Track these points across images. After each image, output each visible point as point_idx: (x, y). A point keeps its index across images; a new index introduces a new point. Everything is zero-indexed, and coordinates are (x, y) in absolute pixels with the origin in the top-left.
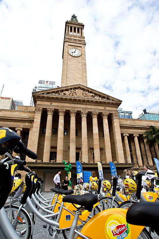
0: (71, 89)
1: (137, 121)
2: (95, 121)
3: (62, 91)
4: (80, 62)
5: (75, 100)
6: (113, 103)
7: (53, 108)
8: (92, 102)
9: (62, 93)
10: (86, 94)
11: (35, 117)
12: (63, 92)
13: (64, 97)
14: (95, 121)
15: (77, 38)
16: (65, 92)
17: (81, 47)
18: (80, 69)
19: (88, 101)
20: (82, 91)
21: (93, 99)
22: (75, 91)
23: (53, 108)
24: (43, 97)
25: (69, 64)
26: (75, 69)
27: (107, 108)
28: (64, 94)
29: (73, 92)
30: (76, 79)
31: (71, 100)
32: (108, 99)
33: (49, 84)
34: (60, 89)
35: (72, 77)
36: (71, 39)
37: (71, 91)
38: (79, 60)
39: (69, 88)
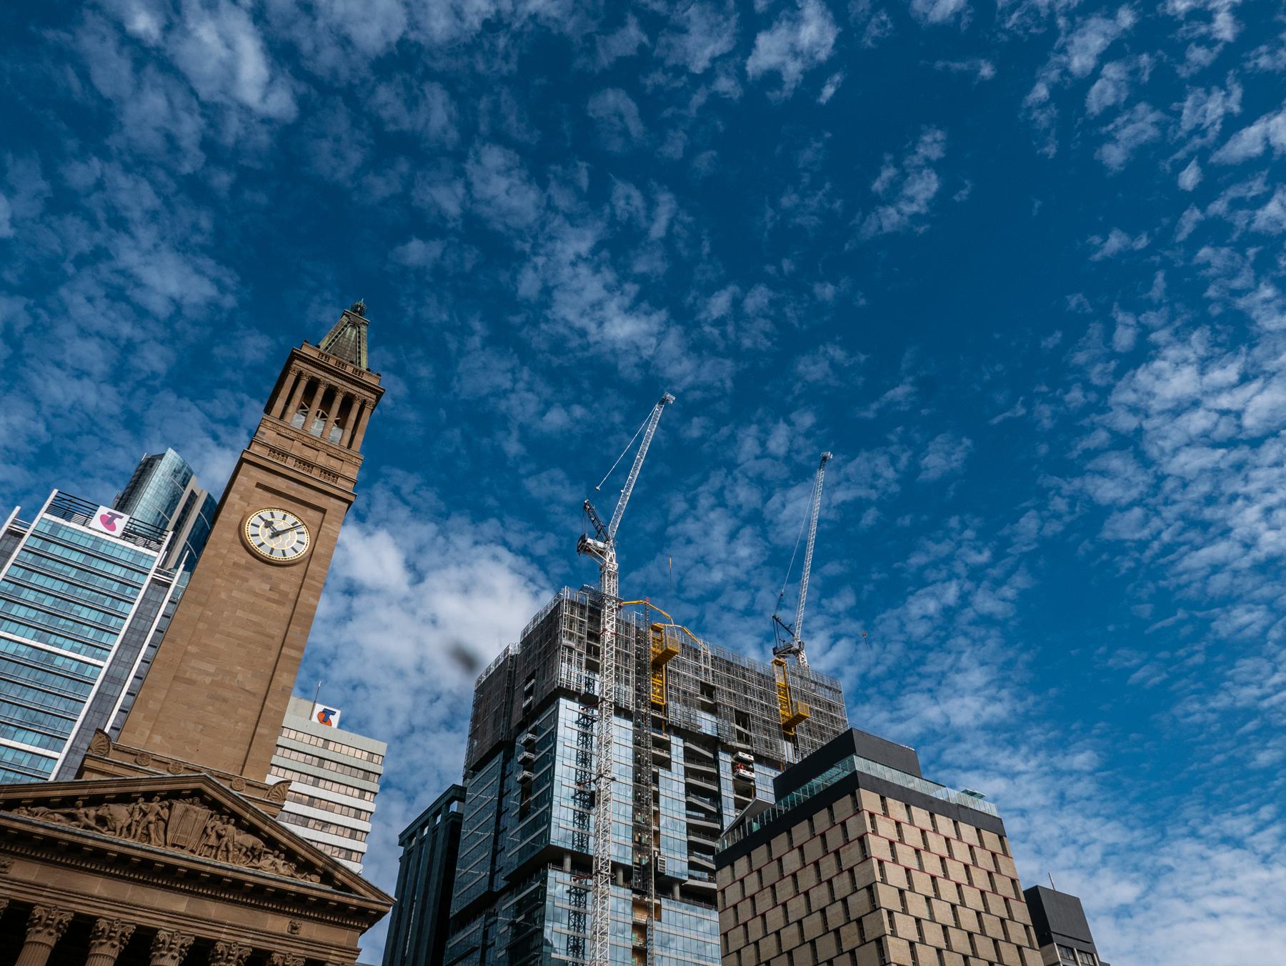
0: (149, 797)
4: (285, 594)
6: (342, 909)
9: (92, 812)
15: (322, 460)
16: (111, 806)
18: (272, 637)
22: (165, 813)
23: (8, 892)
25: (223, 596)
26: (241, 632)
27: (309, 930)
28: (101, 821)
29: (152, 818)
30: (228, 694)
32: (327, 878)
33: (118, 532)
34: (86, 792)
35: (208, 680)
36: (285, 455)
38: (283, 587)
39: (141, 789)
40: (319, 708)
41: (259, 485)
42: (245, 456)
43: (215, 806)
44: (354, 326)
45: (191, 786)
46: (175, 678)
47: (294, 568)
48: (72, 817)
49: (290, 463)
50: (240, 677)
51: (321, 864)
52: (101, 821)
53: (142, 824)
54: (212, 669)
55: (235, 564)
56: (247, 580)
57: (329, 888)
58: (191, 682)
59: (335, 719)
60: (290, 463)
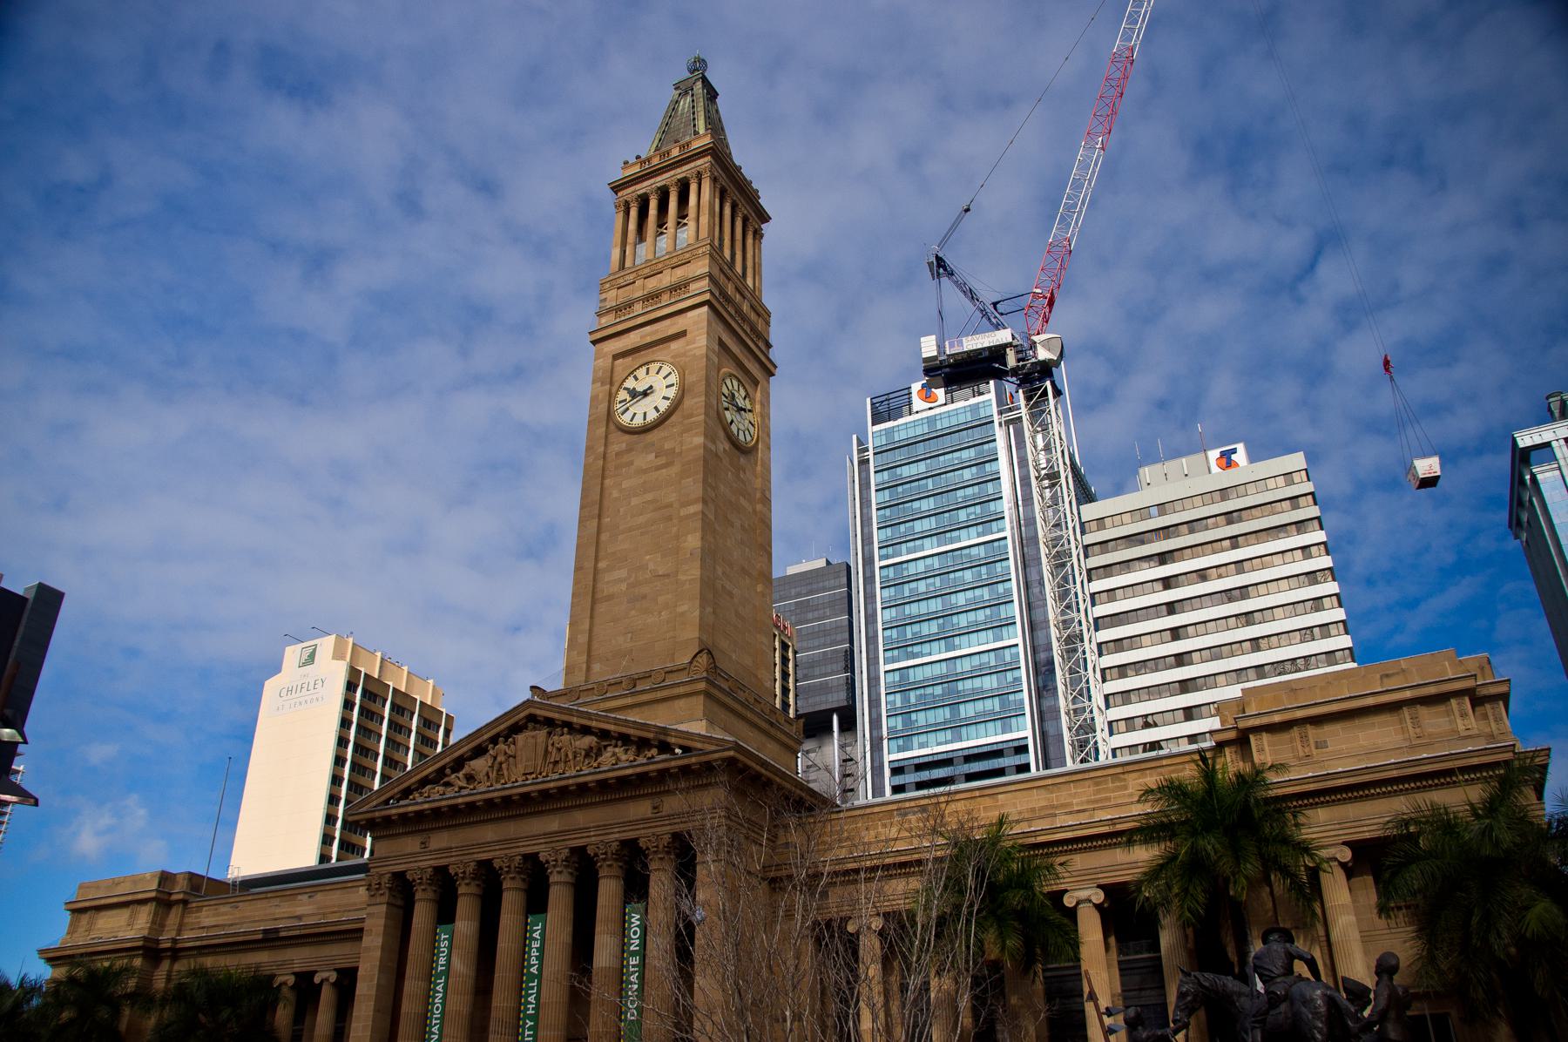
0: (494, 740)
5: (507, 801)
6: (685, 771)
7: (428, 862)
8: (583, 789)
9: (460, 775)
10: (559, 749)
11: (366, 925)
12: (462, 767)
13: (460, 800)
15: (667, 279)
17: (683, 334)
18: (670, 505)
19: (563, 792)
20: (542, 734)
21: (586, 773)
24: (388, 821)
25: (615, 494)
26: (641, 519)
28: (470, 778)
31: (490, 804)
32: (665, 747)
35: (624, 587)
36: (629, 305)
43: (549, 722)
45: (522, 715)
46: (594, 602)
47: (673, 418)
48: (448, 784)
49: (638, 308)
50: (651, 566)
51: (651, 736)
54: (623, 573)
55: (617, 454)
56: (631, 463)
58: (610, 597)
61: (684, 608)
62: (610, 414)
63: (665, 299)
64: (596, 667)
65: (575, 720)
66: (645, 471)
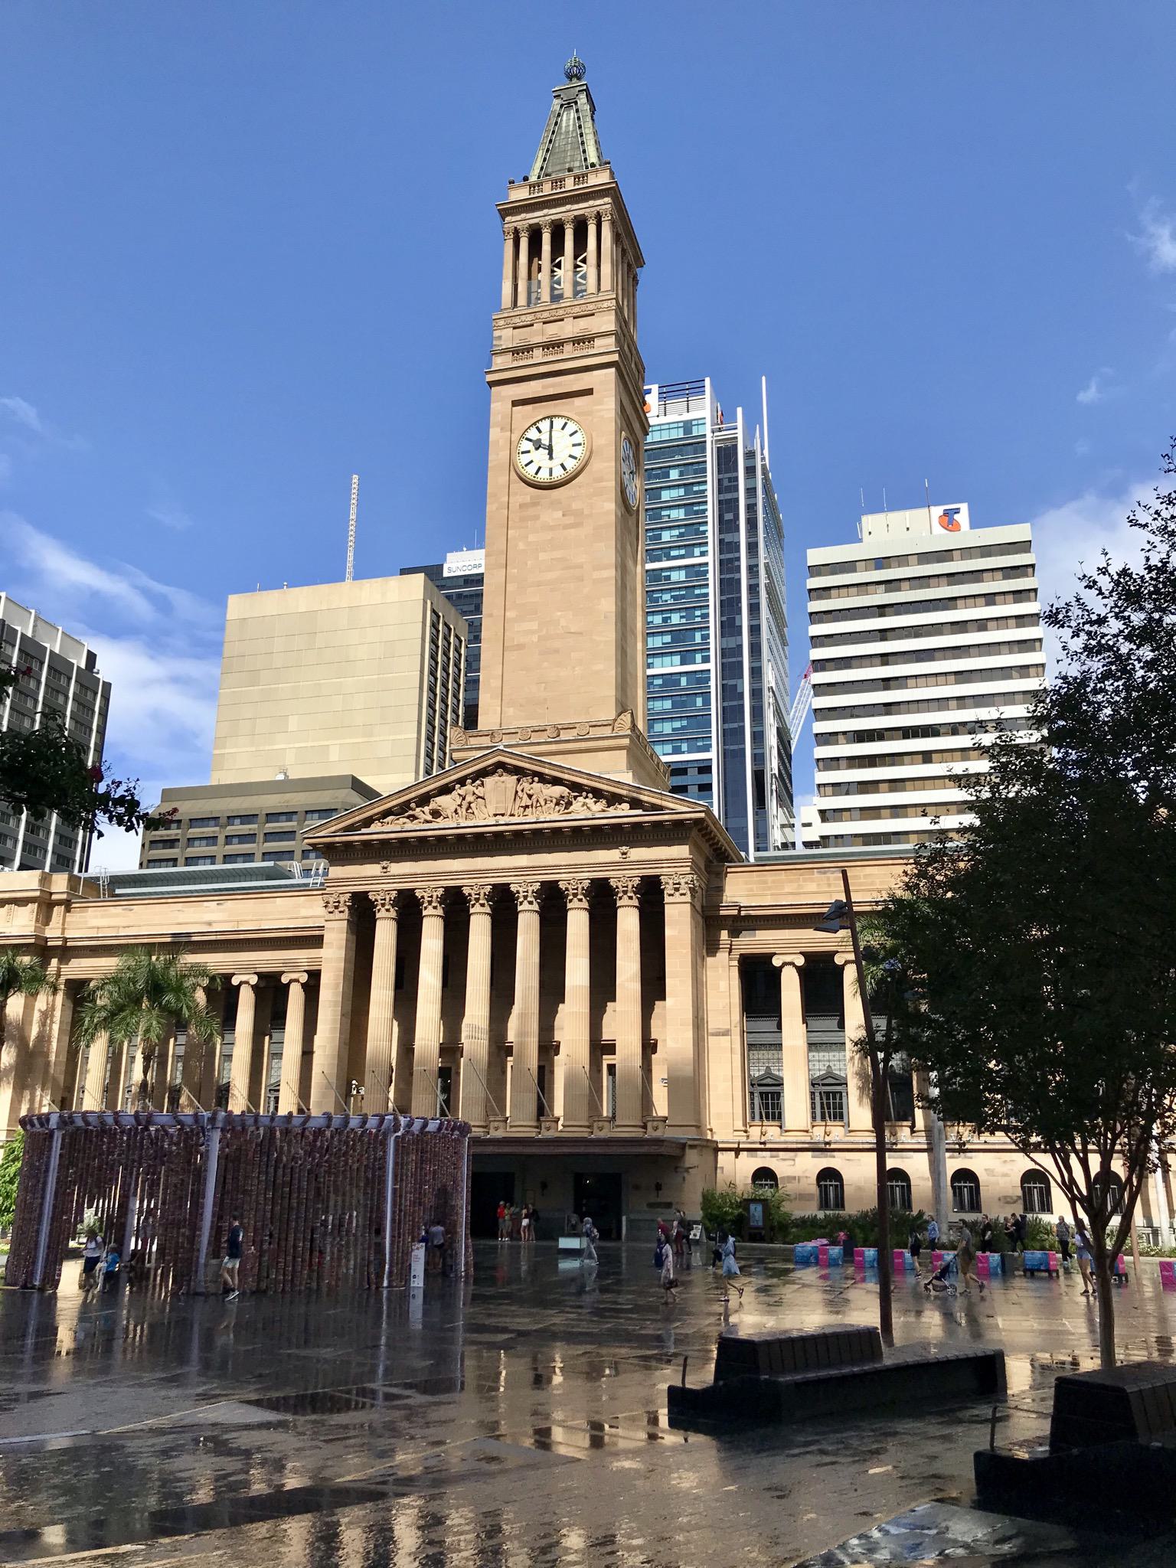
0: (462, 782)
1: (868, 870)
2: (578, 923)
3: (424, 800)
9: (426, 809)
14: (578, 923)
15: (569, 329)
17: (589, 392)
22: (480, 791)
25: (521, 546)
26: (550, 576)
28: (436, 814)
29: (470, 798)
32: (635, 804)
34: (413, 795)
35: (535, 638)
37: (462, 791)
38: (575, 506)
40: (938, 511)
41: (515, 403)
42: (490, 378)
43: (519, 772)
44: (569, 104)
48: (414, 818)
49: (538, 355)
50: (563, 622)
52: (436, 814)
53: (465, 804)
54: (534, 626)
56: (537, 518)
57: (640, 812)
59: (963, 518)
60: (538, 355)
61: (600, 667)
62: (511, 464)
63: (568, 350)
64: (510, 711)
65: (547, 771)
66: (552, 528)
